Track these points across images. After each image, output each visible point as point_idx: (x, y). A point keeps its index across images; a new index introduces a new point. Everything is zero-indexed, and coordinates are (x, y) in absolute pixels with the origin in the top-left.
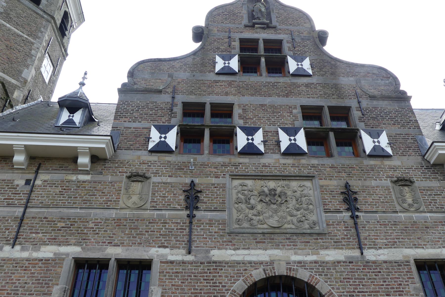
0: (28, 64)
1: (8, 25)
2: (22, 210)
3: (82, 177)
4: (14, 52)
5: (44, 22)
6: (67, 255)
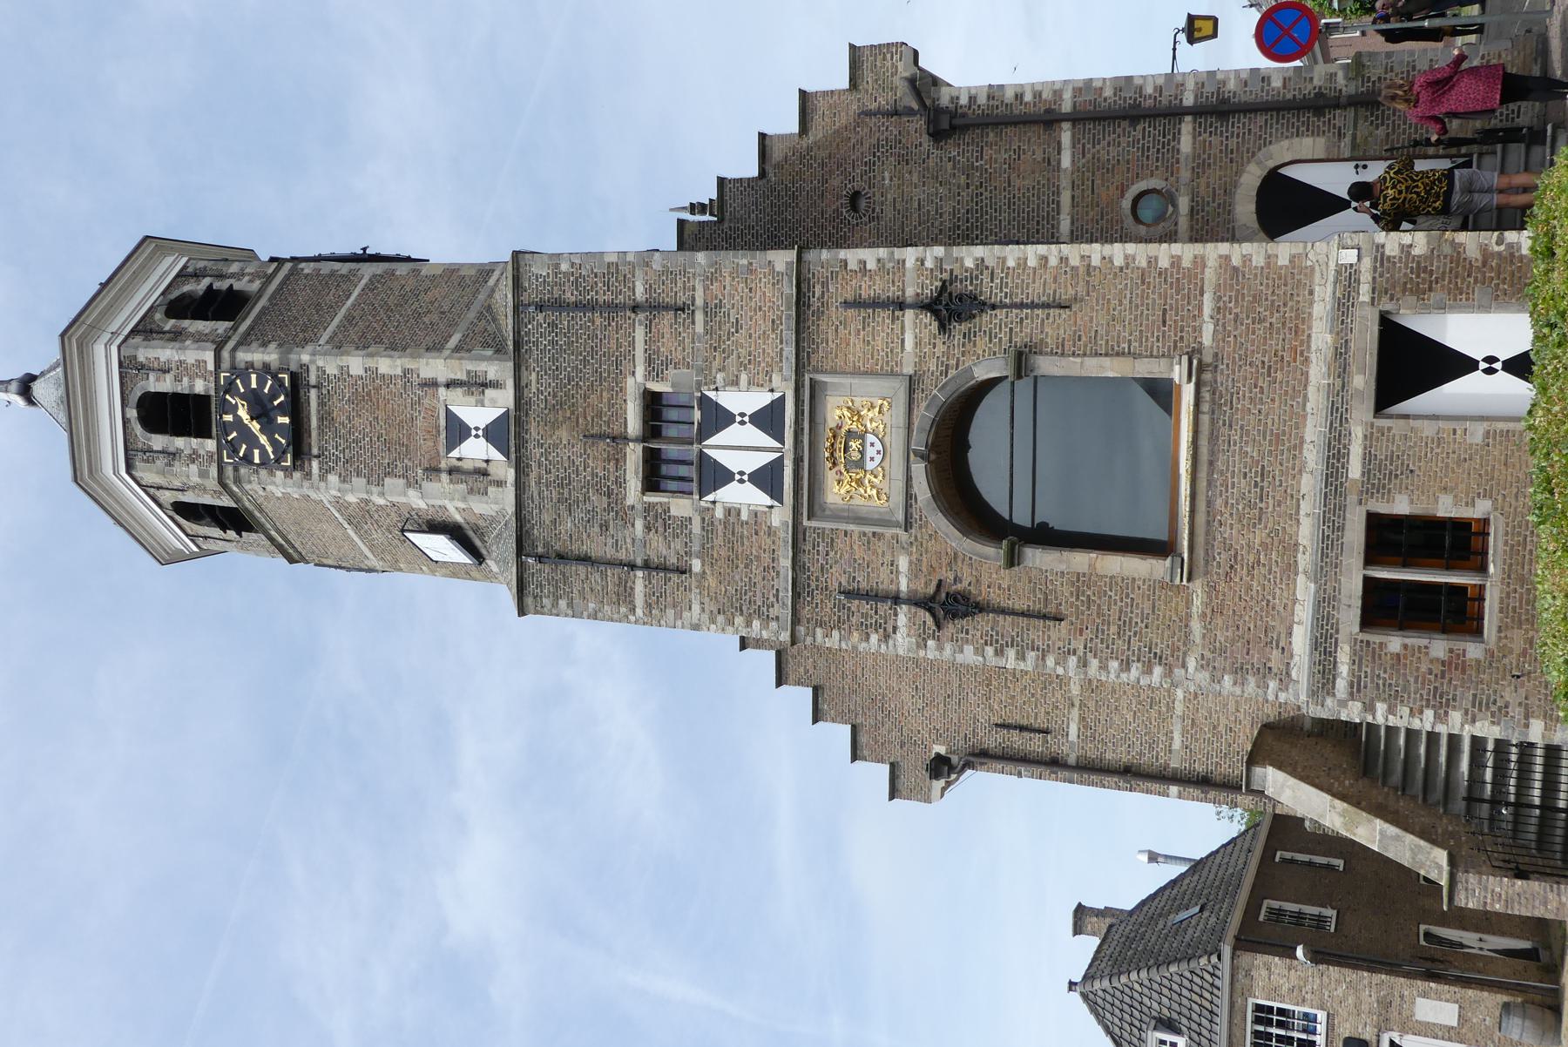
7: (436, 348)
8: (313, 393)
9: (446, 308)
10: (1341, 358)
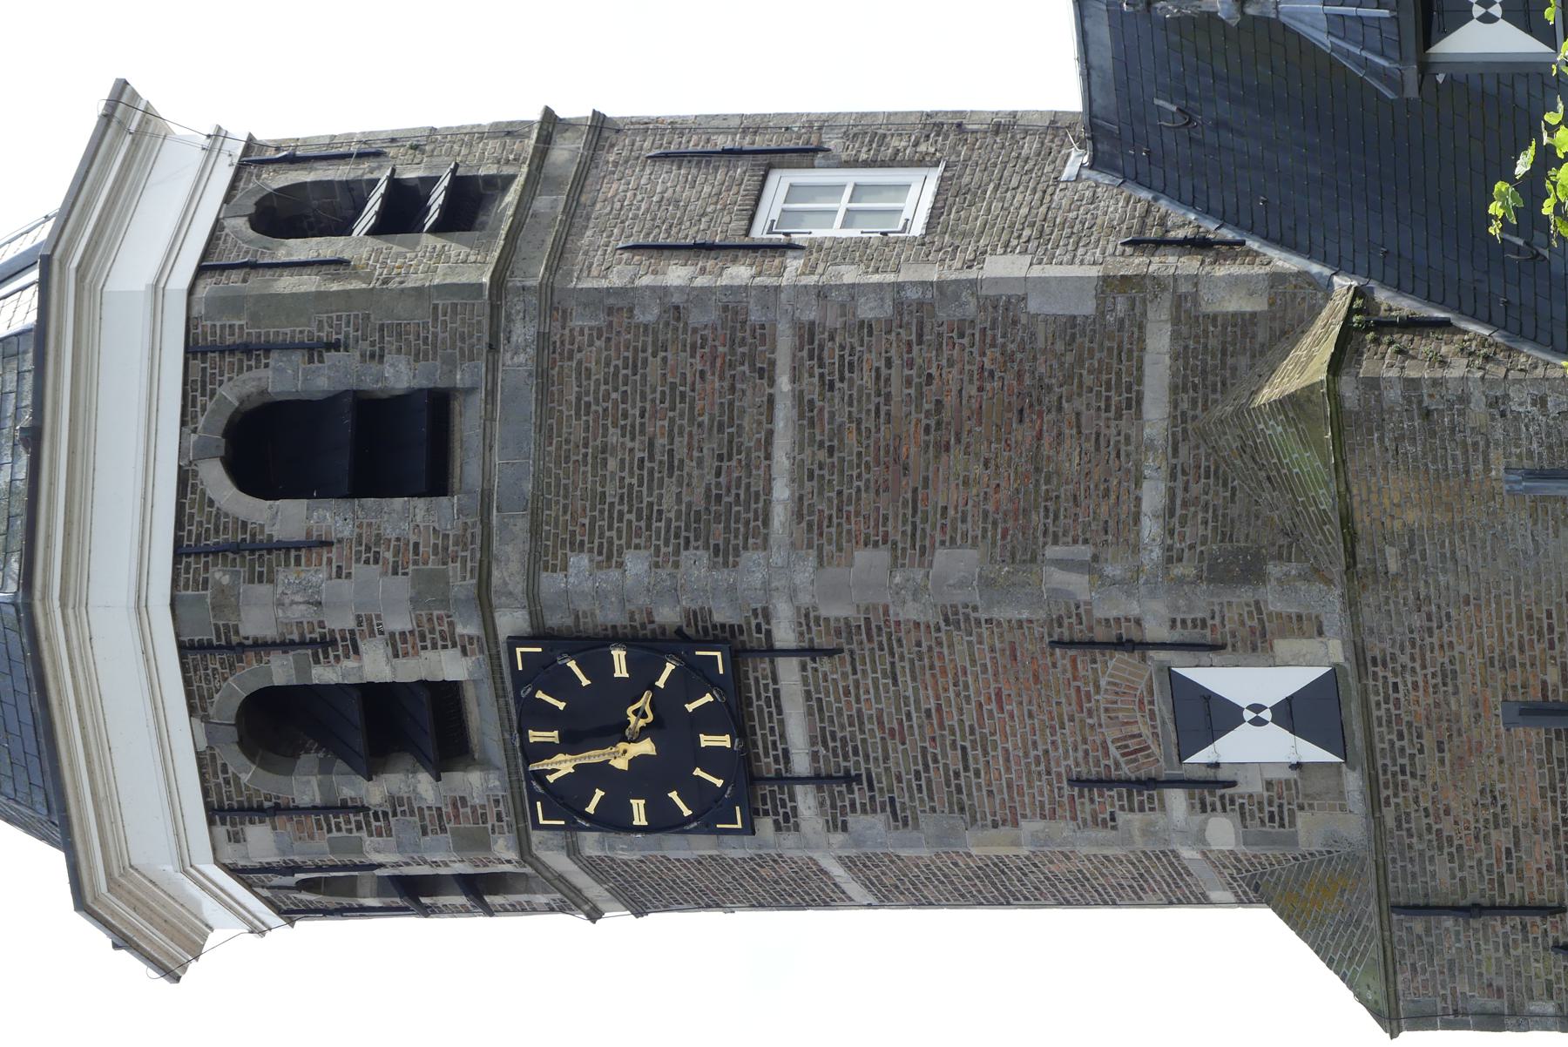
0: (981, 308)
1: (782, 491)
4: (950, 401)
5: (576, 323)
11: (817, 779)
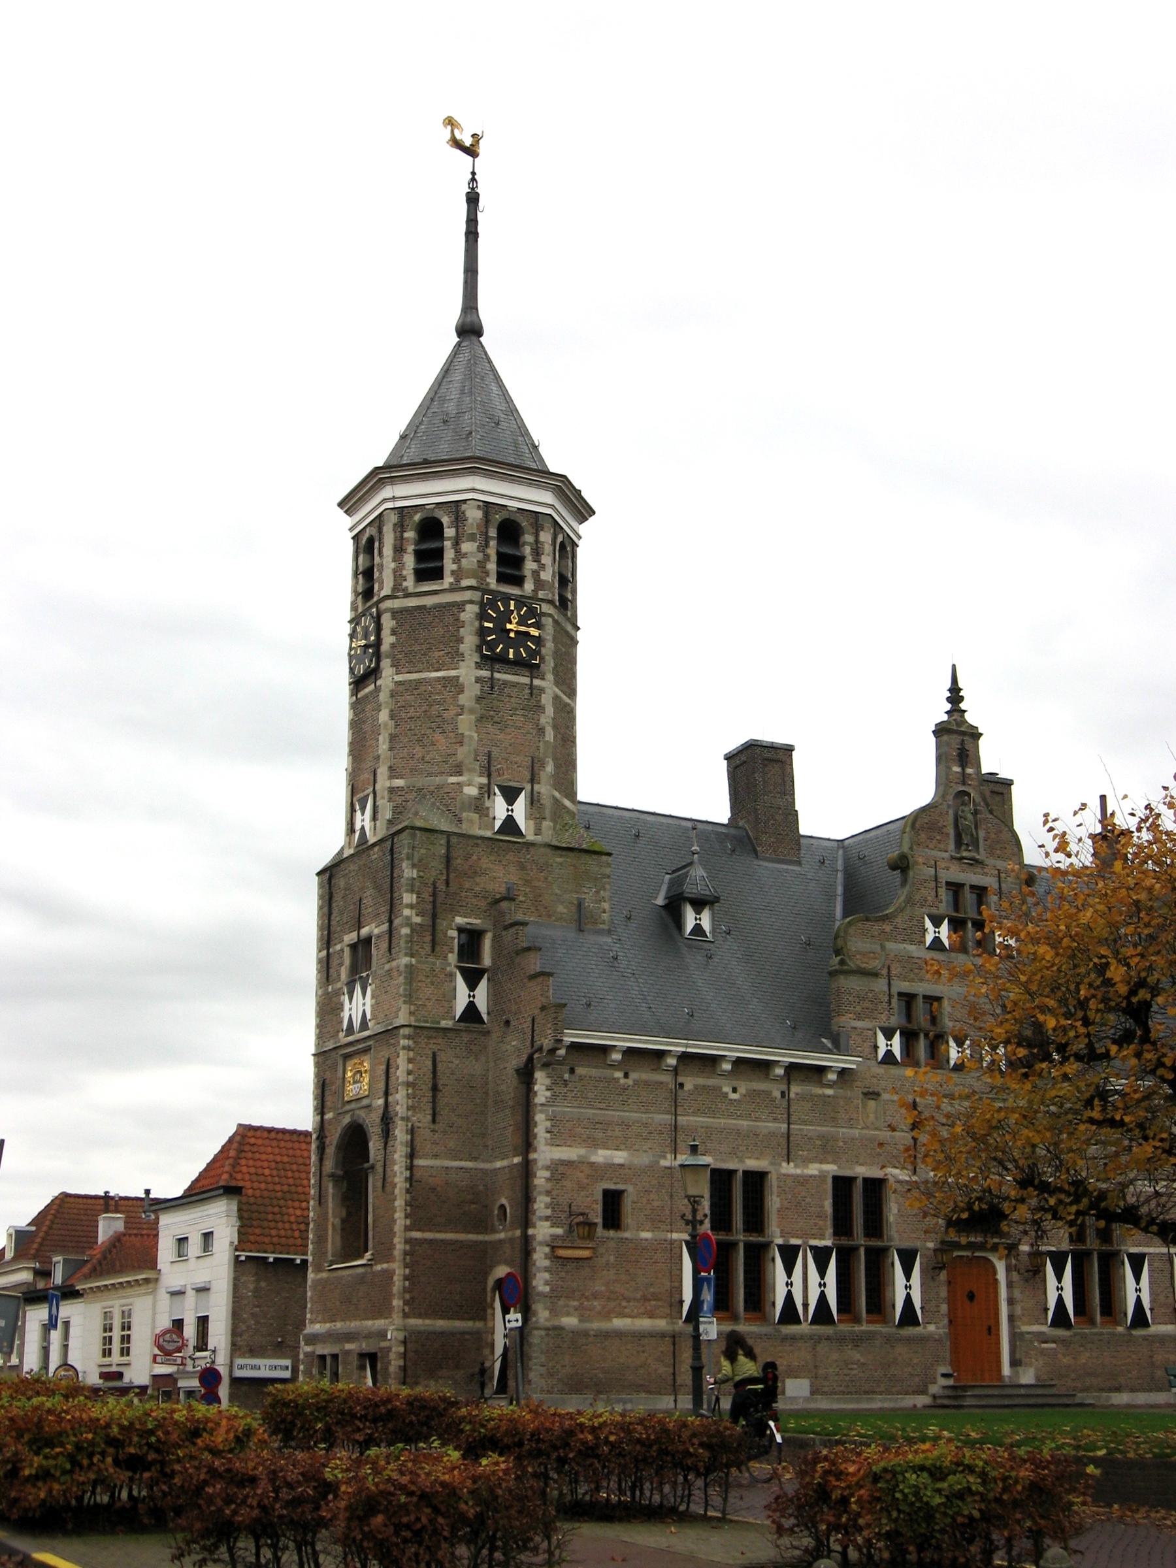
2: (786, 1126)
3: (829, 1092)
6: (828, 1172)
7: (393, 773)
8: (372, 687)
9: (427, 759)
10: (369, 1336)
11: (492, 678)
